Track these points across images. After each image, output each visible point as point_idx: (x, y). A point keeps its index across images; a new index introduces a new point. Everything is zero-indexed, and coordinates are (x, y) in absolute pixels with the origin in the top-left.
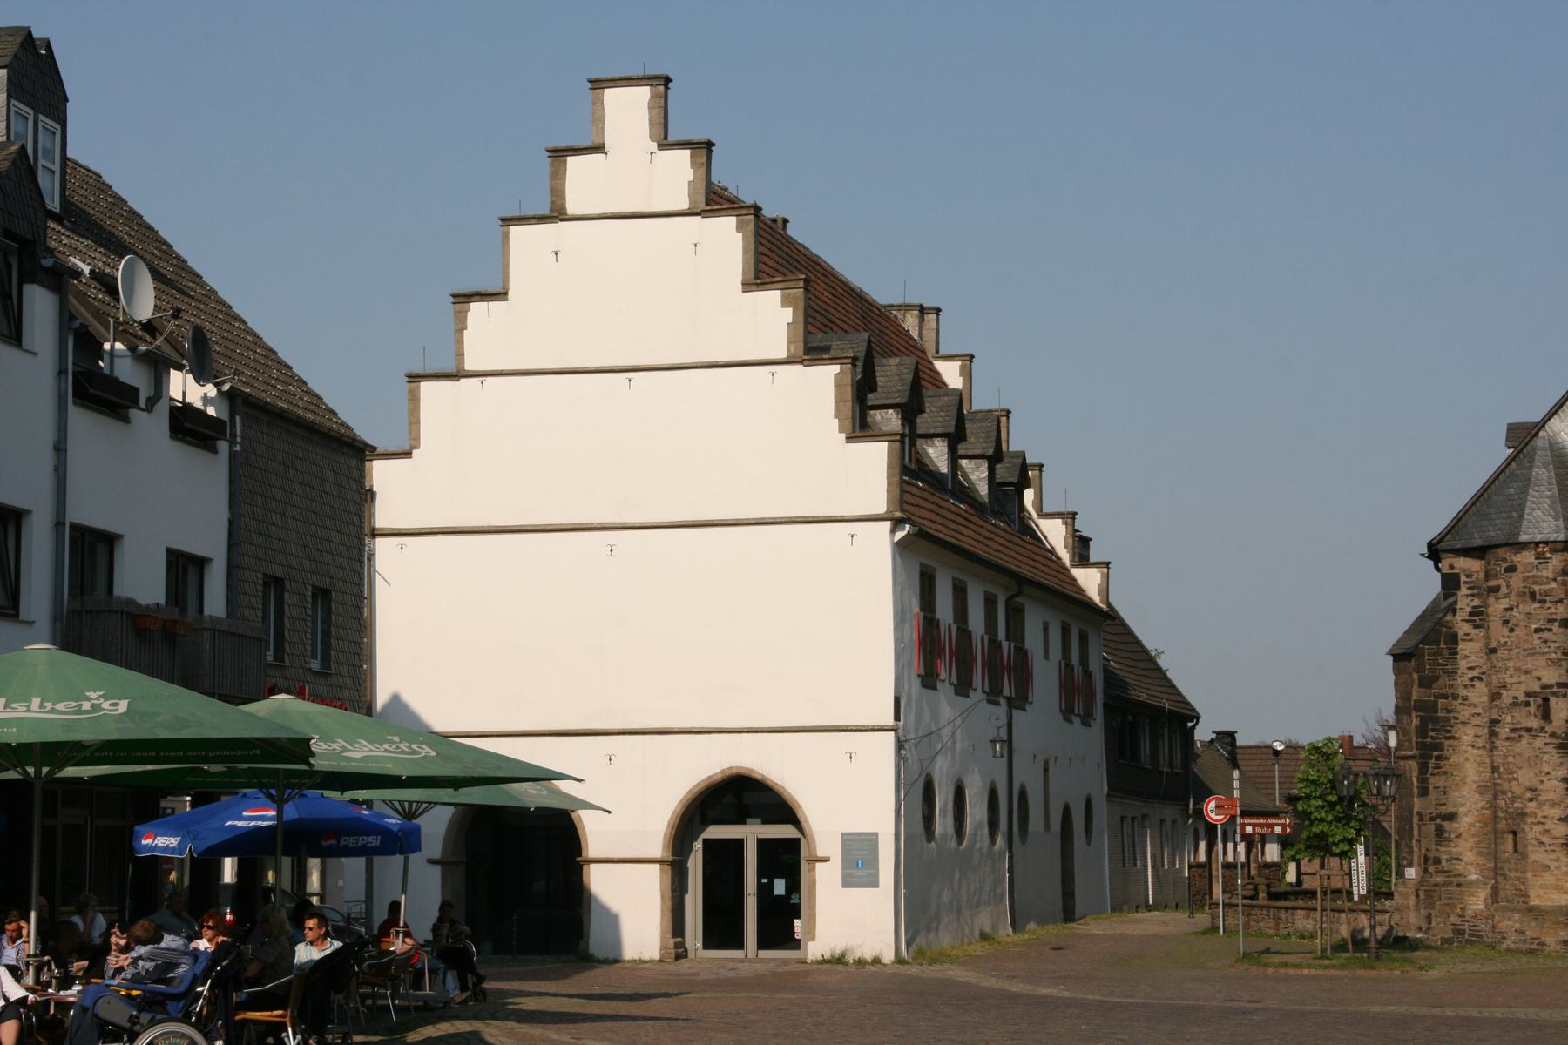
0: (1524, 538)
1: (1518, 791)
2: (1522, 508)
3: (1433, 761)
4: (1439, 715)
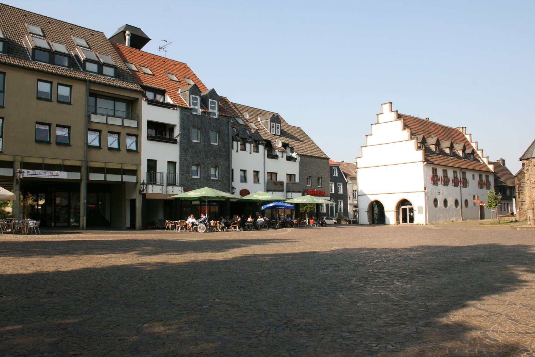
1: (534, 197)
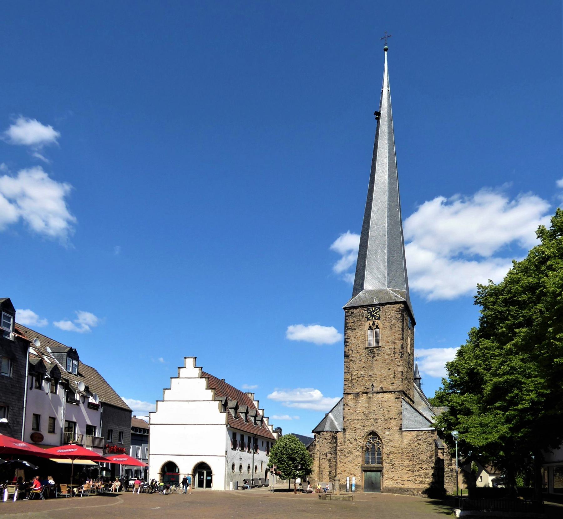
0: (325, 430)
2: (325, 425)
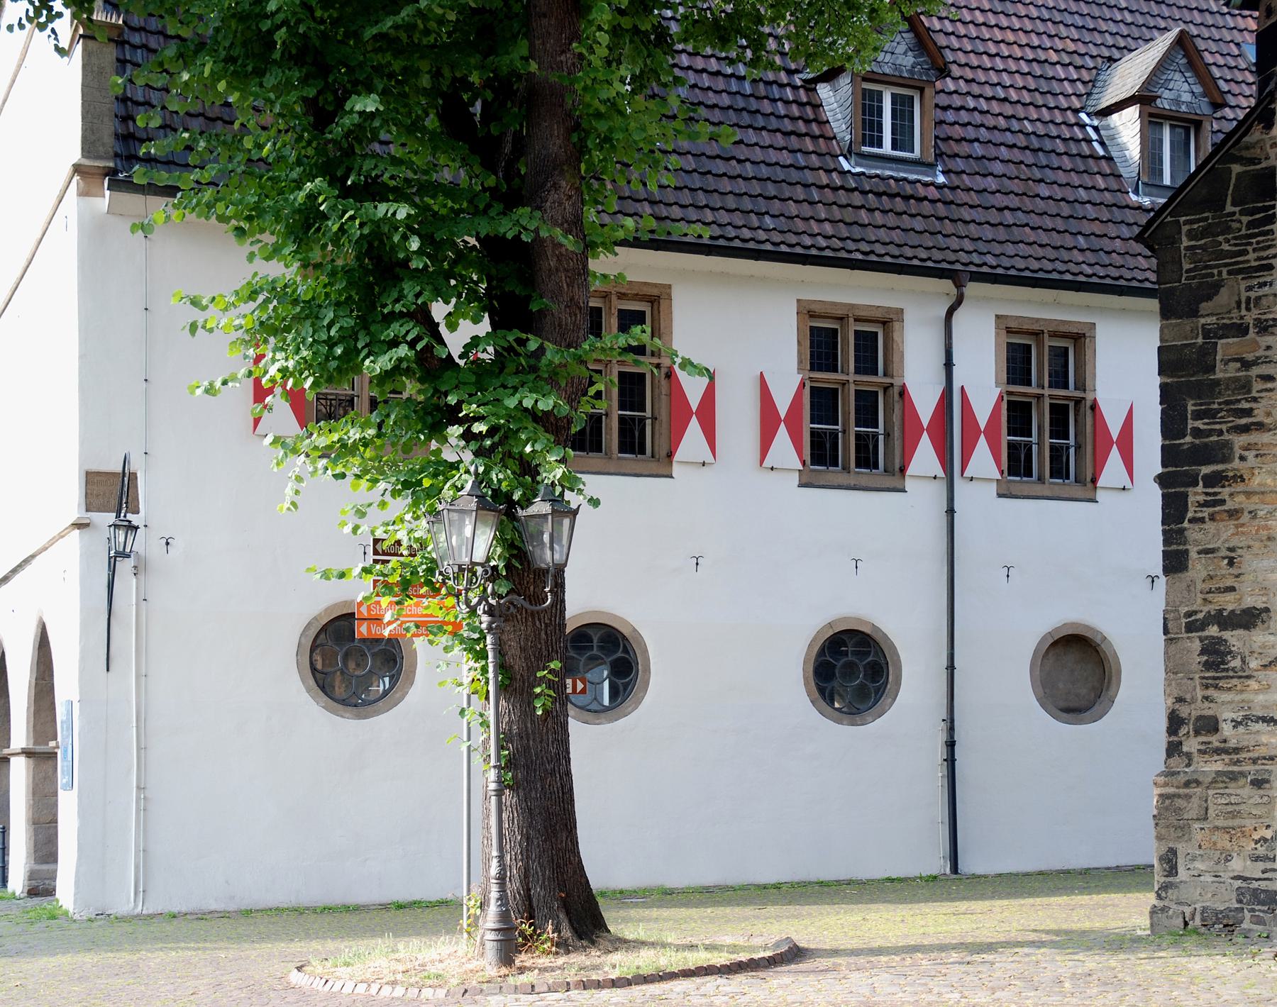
3: (1200, 488)
4: (1219, 375)
